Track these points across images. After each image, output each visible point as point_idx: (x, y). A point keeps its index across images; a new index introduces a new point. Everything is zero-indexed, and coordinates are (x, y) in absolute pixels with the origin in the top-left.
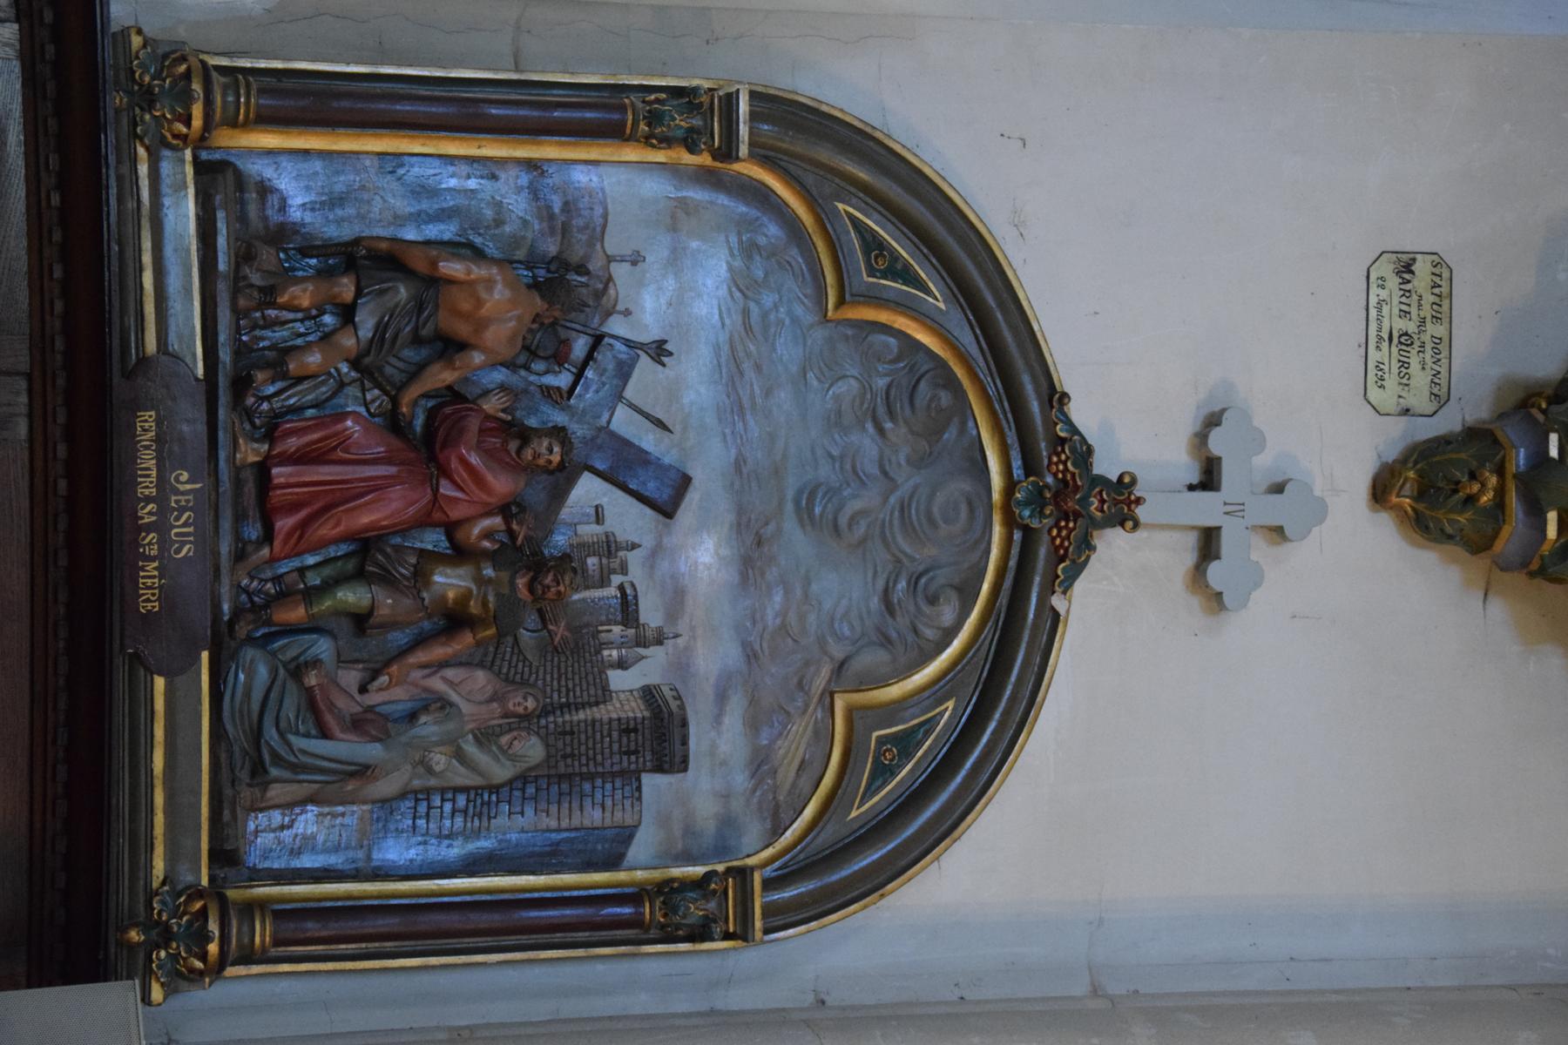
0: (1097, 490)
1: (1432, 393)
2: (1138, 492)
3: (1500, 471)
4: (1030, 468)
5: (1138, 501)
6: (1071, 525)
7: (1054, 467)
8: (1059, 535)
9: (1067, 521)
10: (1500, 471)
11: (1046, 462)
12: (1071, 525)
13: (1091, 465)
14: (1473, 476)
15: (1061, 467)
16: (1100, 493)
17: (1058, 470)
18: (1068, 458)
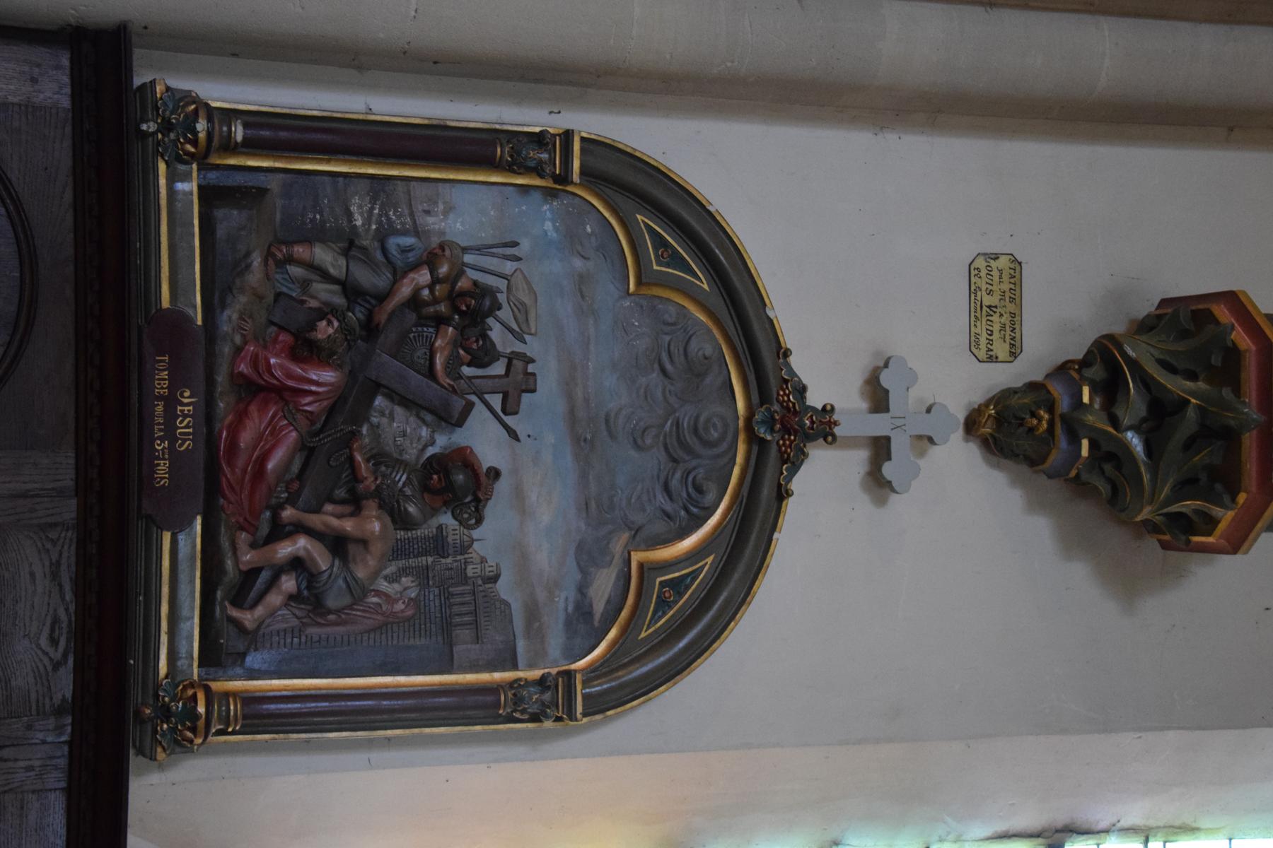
0: (809, 415)
1: (1010, 352)
2: (835, 417)
3: (1051, 409)
4: (764, 398)
5: (836, 423)
6: (792, 438)
7: (781, 398)
8: (784, 444)
9: (790, 435)
10: (1051, 409)
11: (775, 396)
12: (792, 438)
13: (805, 398)
14: (1033, 415)
15: (786, 398)
16: (811, 416)
17: (784, 401)
18: (790, 392)
